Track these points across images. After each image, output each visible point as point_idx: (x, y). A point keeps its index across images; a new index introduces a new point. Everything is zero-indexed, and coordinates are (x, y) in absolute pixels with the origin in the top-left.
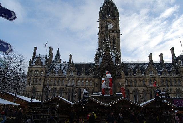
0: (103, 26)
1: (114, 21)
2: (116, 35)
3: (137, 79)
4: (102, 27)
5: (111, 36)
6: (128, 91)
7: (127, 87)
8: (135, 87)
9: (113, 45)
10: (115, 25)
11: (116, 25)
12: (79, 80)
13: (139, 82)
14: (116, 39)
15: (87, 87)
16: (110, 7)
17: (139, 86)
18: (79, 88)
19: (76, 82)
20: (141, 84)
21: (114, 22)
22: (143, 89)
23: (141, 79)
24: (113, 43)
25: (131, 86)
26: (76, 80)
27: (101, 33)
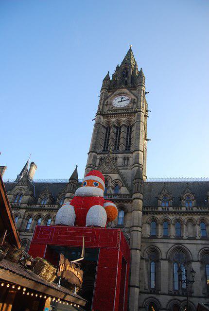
1: (134, 92)
2: (134, 118)
3: (184, 218)
4: (106, 103)
5: (124, 119)
6: (155, 251)
7: (154, 240)
8: (177, 241)
10: (134, 97)
11: (137, 97)
12: (30, 216)
13: (190, 225)
14: (133, 125)
17: (189, 239)
18: (25, 237)
19: (22, 223)
20: (194, 231)
21: (134, 94)
22: (203, 246)
23: (196, 218)
25: (166, 237)
27: (101, 114)
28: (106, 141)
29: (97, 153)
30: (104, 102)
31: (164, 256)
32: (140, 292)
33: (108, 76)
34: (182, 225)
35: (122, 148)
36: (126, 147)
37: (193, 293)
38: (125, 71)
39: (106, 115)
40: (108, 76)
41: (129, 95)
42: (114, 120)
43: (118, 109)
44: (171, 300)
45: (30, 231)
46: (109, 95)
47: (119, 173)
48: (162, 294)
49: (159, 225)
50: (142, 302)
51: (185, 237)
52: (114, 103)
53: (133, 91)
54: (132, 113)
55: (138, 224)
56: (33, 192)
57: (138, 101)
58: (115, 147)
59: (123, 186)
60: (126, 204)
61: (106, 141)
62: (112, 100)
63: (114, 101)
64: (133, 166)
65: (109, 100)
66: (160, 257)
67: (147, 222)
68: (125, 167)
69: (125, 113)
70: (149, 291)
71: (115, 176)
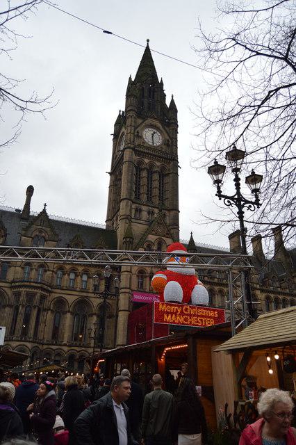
1: (167, 128)
5: (158, 164)
9: (158, 186)
10: (168, 138)
11: (171, 139)
14: (167, 175)
15: (85, 294)
16: (156, 89)
19: (53, 277)
28: (138, 187)
34: (215, 295)
39: (138, 151)
41: (162, 131)
42: (147, 161)
43: (149, 148)
45: (65, 288)
54: (167, 159)
61: (138, 187)
62: (143, 129)
65: (139, 129)
69: (161, 157)
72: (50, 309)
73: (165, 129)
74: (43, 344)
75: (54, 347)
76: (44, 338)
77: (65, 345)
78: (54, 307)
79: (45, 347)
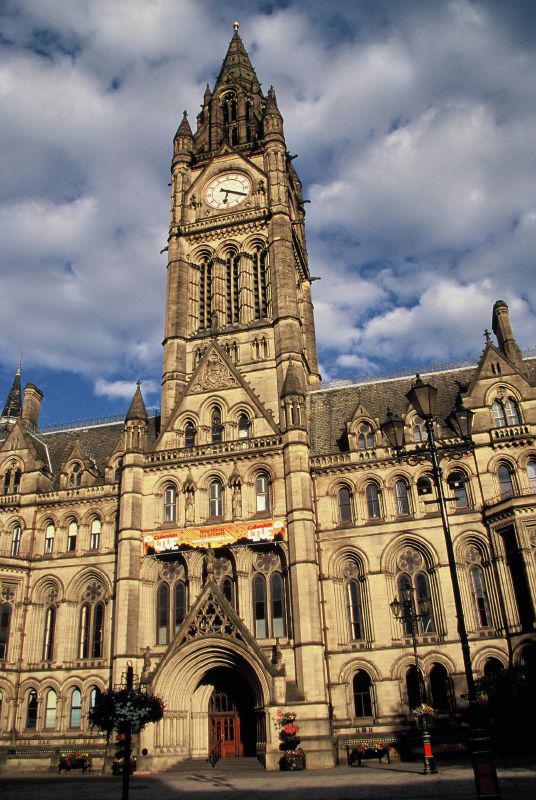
0: (194, 197)
1: (258, 160)
5: (240, 238)
7: (348, 533)
10: (258, 176)
11: (265, 174)
15: (92, 560)
19: (33, 539)
24: (256, 276)
26: (30, 526)
29: (185, 339)
30: (184, 200)
31: (372, 564)
32: (327, 654)
33: (185, 123)
35: (248, 316)
36: (257, 311)
37: (445, 634)
38: (229, 103)
40: (185, 123)
42: (215, 244)
44: (399, 659)
45: (55, 556)
46: (193, 180)
47: (243, 385)
48: (379, 649)
49: (357, 495)
50: (338, 671)
51: (418, 515)
52: (209, 200)
53: (254, 160)
55: (304, 504)
56: (44, 459)
57: (269, 184)
58: (230, 316)
59: (256, 417)
60: (269, 460)
63: (209, 192)
64: (279, 360)
66: (367, 571)
67: (327, 494)
68: (259, 365)
70: (350, 647)
71: (236, 396)
72: (30, 603)
73: (254, 166)
74: (19, 671)
75: (40, 675)
76: (21, 660)
77: (59, 668)
78: (39, 598)
79: (24, 676)
